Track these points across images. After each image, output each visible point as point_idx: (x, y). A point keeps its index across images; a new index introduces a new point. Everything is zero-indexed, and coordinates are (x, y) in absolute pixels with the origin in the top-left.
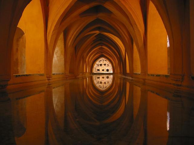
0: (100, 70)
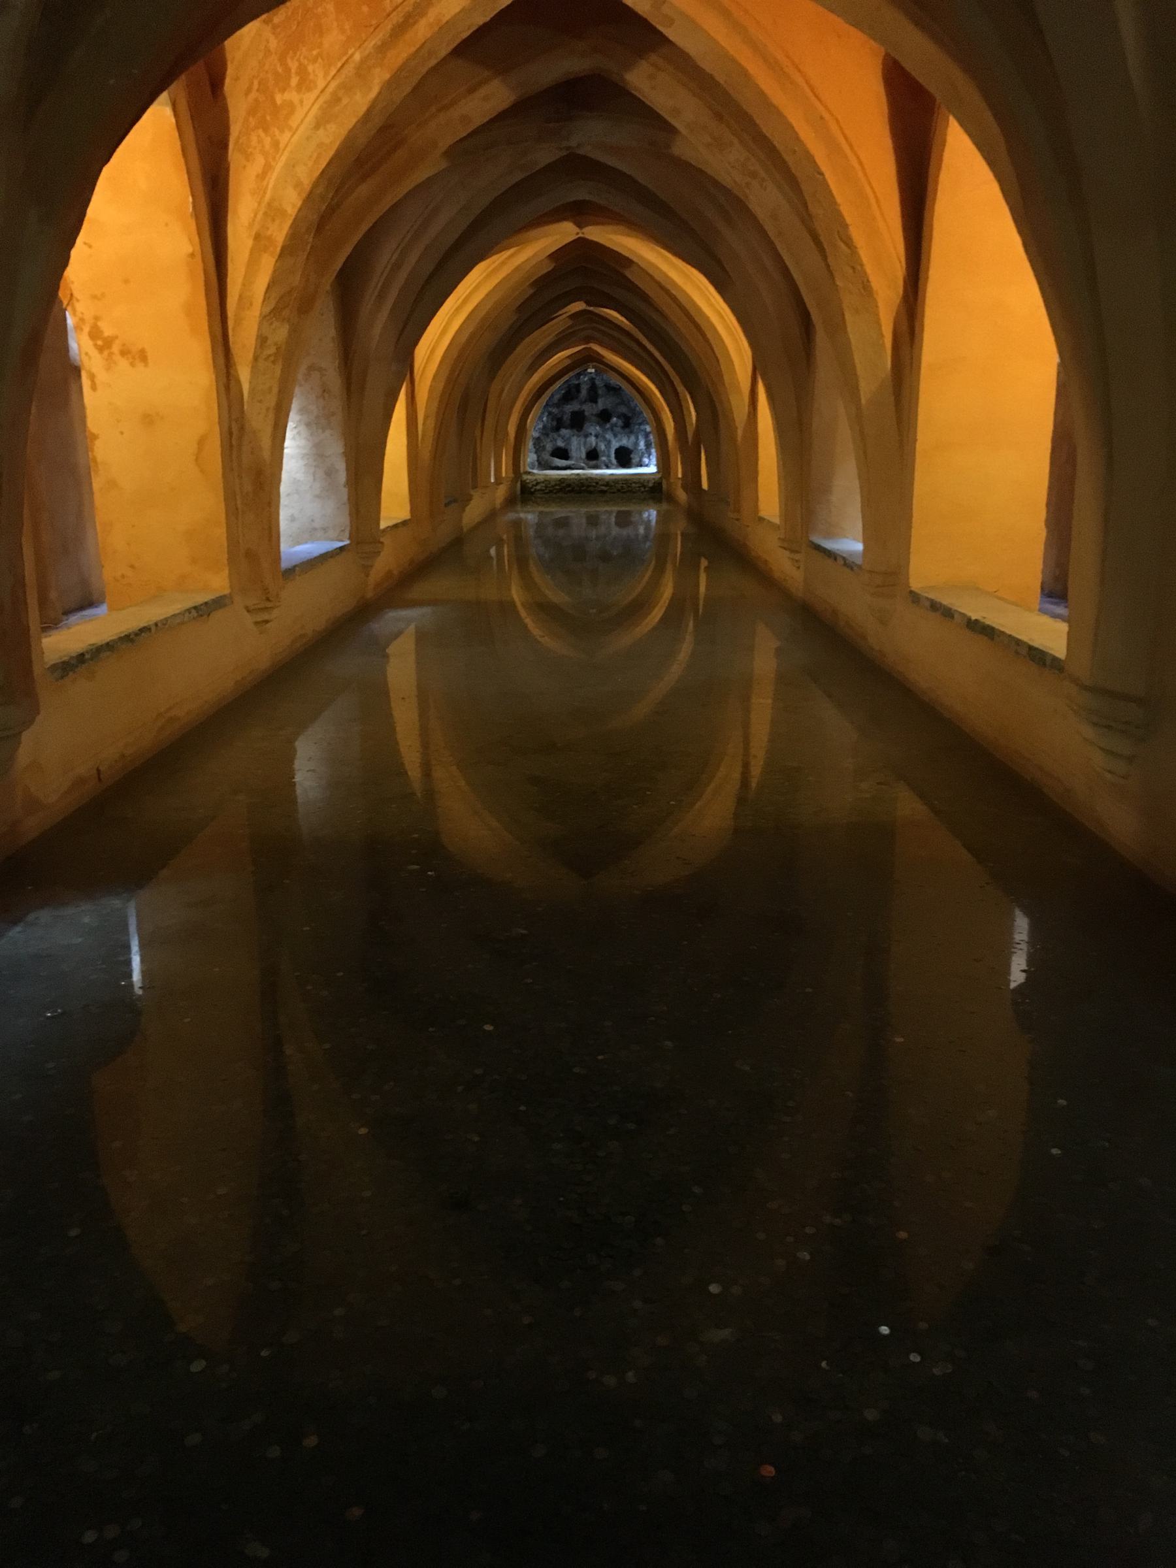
0: (574, 453)
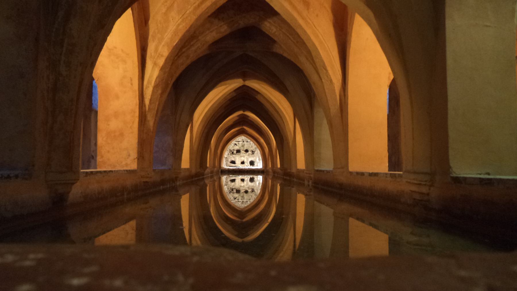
0: (237, 162)
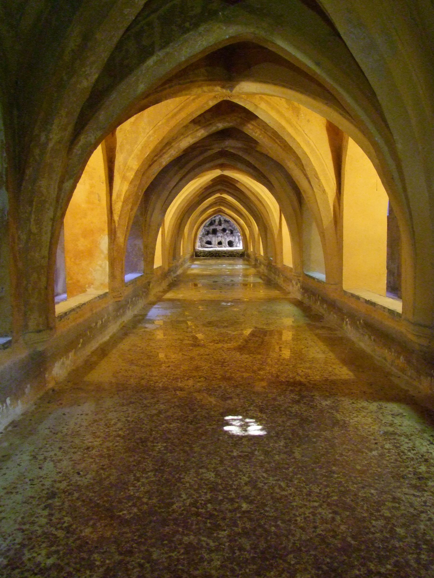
0: (213, 243)
